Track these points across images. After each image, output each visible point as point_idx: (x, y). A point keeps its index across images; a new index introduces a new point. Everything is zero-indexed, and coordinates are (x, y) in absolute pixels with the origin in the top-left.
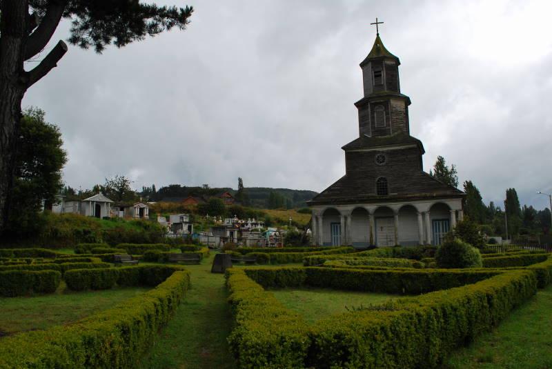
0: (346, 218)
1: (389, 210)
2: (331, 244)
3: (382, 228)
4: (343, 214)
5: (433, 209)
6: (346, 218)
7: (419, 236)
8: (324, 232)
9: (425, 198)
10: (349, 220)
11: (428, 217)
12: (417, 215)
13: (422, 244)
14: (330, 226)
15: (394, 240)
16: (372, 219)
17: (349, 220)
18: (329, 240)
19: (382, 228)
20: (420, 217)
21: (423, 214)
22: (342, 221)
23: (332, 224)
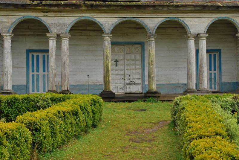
0: (59, 38)
1: (140, 28)
2: (26, 87)
3: (116, 61)
4: (54, 30)
5: (212, 29)
6: (59, 38)
7: (189, 76)
8: (13, 67)
9: (203, 9)
10: (65, 43)
11: (203, 44)
12: (187, 38)
13: (194, 88)
14: (25, 55)
15: (139, 81)
16: (107, 43)
17: (65, 43)
18: (23, 81)
19: (116, 61)
20: (192, 43)
21: (197, 37)
22: (52, 44)
23: (28, 51)
